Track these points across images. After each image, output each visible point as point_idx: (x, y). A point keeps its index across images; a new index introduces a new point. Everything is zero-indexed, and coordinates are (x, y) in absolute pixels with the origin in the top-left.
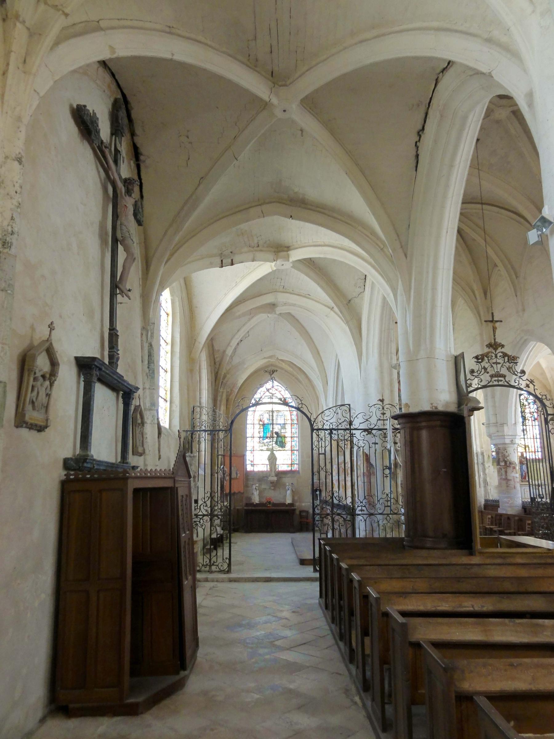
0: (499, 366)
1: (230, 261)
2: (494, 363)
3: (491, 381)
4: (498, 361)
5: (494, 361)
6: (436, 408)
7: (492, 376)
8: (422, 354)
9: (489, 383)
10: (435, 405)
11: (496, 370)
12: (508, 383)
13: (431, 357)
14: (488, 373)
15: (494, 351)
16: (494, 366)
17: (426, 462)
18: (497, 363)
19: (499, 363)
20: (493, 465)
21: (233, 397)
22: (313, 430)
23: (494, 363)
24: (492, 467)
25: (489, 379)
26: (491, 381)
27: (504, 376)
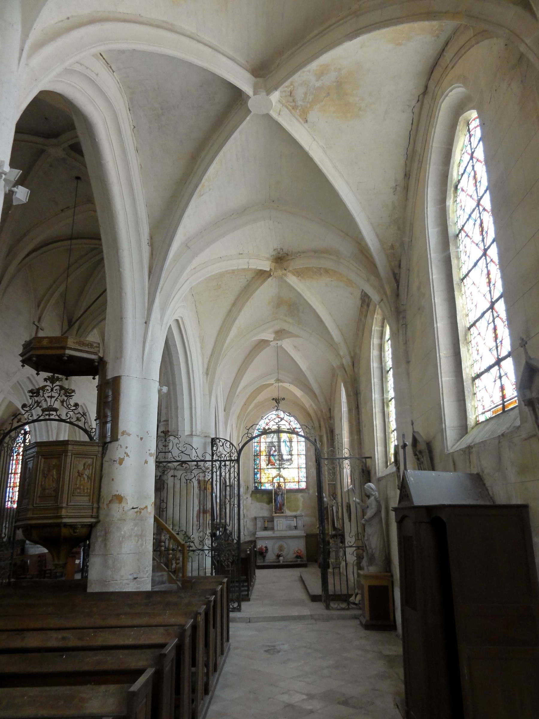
0: (53, 400)
2: (48, 397)
3: (42, 415)
4: (53, 394)
5: (50, 394)
7: (43, 410)
9: (40, 417)
11: (49, 404)
12: (59, 416)
14: (40, 407)
15: (51, 385)
16: (48, 400)
18: (51, 397)
19: (54, 397)
20: (251, 496)
23: (48, 397)
24: (250, 498)
25: (40, 413)
26: (42, 415)
27: (56, 410)
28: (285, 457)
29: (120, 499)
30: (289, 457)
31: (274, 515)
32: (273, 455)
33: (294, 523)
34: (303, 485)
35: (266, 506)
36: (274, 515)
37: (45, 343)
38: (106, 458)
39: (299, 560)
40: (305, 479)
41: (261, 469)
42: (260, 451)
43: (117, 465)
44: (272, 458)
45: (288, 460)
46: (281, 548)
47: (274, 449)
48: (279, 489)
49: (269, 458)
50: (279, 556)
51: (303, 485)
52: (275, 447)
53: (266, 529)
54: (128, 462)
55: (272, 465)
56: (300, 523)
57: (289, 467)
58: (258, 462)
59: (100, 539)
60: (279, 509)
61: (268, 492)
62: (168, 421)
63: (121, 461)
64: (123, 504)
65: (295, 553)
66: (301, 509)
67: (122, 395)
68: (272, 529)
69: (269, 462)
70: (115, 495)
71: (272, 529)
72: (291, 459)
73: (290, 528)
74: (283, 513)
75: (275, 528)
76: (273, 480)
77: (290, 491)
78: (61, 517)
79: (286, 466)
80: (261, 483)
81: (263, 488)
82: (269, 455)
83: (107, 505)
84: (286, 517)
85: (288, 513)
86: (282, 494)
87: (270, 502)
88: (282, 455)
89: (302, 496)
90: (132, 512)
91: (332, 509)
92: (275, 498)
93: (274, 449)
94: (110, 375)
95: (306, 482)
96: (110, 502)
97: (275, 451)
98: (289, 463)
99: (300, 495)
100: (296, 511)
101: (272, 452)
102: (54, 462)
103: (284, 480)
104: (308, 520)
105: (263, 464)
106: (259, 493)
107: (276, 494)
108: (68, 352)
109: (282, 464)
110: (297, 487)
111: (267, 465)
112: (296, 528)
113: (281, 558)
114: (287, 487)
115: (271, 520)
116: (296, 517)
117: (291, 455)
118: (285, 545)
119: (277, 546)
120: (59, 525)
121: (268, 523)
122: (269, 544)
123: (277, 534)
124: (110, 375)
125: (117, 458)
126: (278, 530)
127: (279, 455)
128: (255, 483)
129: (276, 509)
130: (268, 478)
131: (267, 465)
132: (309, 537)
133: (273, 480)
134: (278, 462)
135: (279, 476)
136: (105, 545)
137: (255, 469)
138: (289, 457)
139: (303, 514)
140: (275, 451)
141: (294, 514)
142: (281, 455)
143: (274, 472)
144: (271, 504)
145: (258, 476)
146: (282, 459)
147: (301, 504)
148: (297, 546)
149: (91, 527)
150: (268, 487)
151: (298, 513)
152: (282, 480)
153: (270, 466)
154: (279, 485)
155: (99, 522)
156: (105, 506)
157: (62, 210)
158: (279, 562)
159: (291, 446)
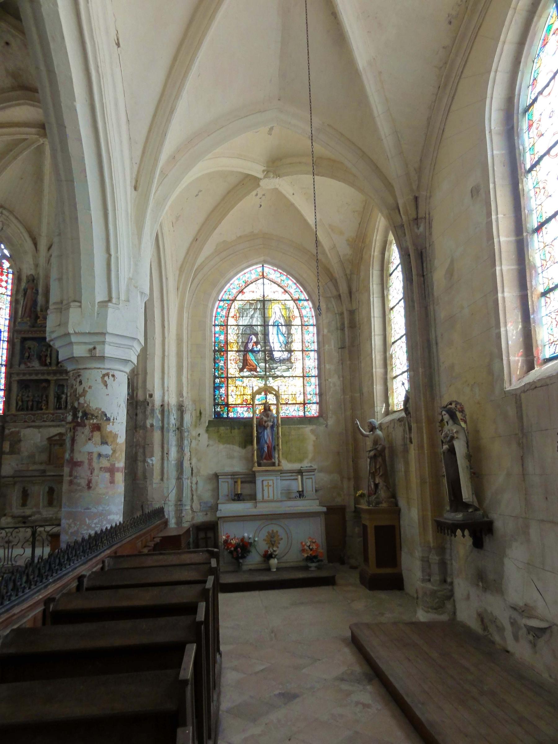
20: (207, 431)
24: (206, 436)
28: (277, 355)
30: (286, 355)
31: (256, 468)
32: (252, 351)
33: (296, 486)
34: (313, 410)
35: (237, 451)
36: (256, 468)
39: (313, 565)
40: (316, 399)
41: (227, 378)
42: (226, 343)
44: (251, 356)
45: (282, 361)
46: (272, 539)
47: (254, 339)
48: (267, 416)
49: (245, 356)
50: (268, 556)
51: (313, 410)
52: (256, 335)
53: (238, 498)
55: (250, 370)
56: (309, 485)
57: (285, 374)
58: (222, 364)
60: (267, 456)
61: (244, 424)
65: (303, 551)
66: (310, 456)
68: (253, 497)
69: (245, 364)
71: (253, 497)
72: (289, 360)
73: (288, 495)
74: (273, 464)
75: (259, 496)
76: (253, 399)
77: (288, 420)
79: (278, 373)
80: (227, 405)
81: (231, 415)
82: (245, 351)
84: (282, 472)
85: (286, 465)
86: (272, 427)
87: (247, 442)
88: (271, 352)
89: (312, 431)
91: (452, 451)
92: (258, 436)
93: (254, 339)
95: (320, 403)
97: (256, 343)
98: (284, 367)
99: (307, 429)
100: (301, 461)
101: (250, 346)
103: (277, 396)
104: (323, 478)
105: (233, 369)
106: (221, 423)
107: (261, 425)
109: (271, 369)
110: (301, 414)
111: (241, 370)
112: (301, 494)
113: (274, 562)
114: (282, 414)
115: (250, 478)
116: (300, 472)
117: (290, 351)
118: (282, 533)
119: (264, 534)
121: (244, 487)
122: (247, 532)
123: (263, 508)
126: (264, 501)
127: (264, 351)
128: (216, 405)
129: (260, 457)
130: (241, 394)
131: (241, 370)
132: (335, 517)
133: (253, 399)
134: (262, 365)
135: (267, 390)
137: (215, 377)
138: (286, 355)
139: (315, 467)
140: (256, 343)
141: (296, 466)
142: (269, 353)
143: (257, 384)
144: (249, 447)
145: (223, 391)
146: (272, 358)
147: (310, 447)
148: (306, 536)
150: (243, 413)
151: (305, 464)
152: (271, 399)
153: (246, 373)
154: (267, 408)
158: (268, 569)
159: (289, 334)
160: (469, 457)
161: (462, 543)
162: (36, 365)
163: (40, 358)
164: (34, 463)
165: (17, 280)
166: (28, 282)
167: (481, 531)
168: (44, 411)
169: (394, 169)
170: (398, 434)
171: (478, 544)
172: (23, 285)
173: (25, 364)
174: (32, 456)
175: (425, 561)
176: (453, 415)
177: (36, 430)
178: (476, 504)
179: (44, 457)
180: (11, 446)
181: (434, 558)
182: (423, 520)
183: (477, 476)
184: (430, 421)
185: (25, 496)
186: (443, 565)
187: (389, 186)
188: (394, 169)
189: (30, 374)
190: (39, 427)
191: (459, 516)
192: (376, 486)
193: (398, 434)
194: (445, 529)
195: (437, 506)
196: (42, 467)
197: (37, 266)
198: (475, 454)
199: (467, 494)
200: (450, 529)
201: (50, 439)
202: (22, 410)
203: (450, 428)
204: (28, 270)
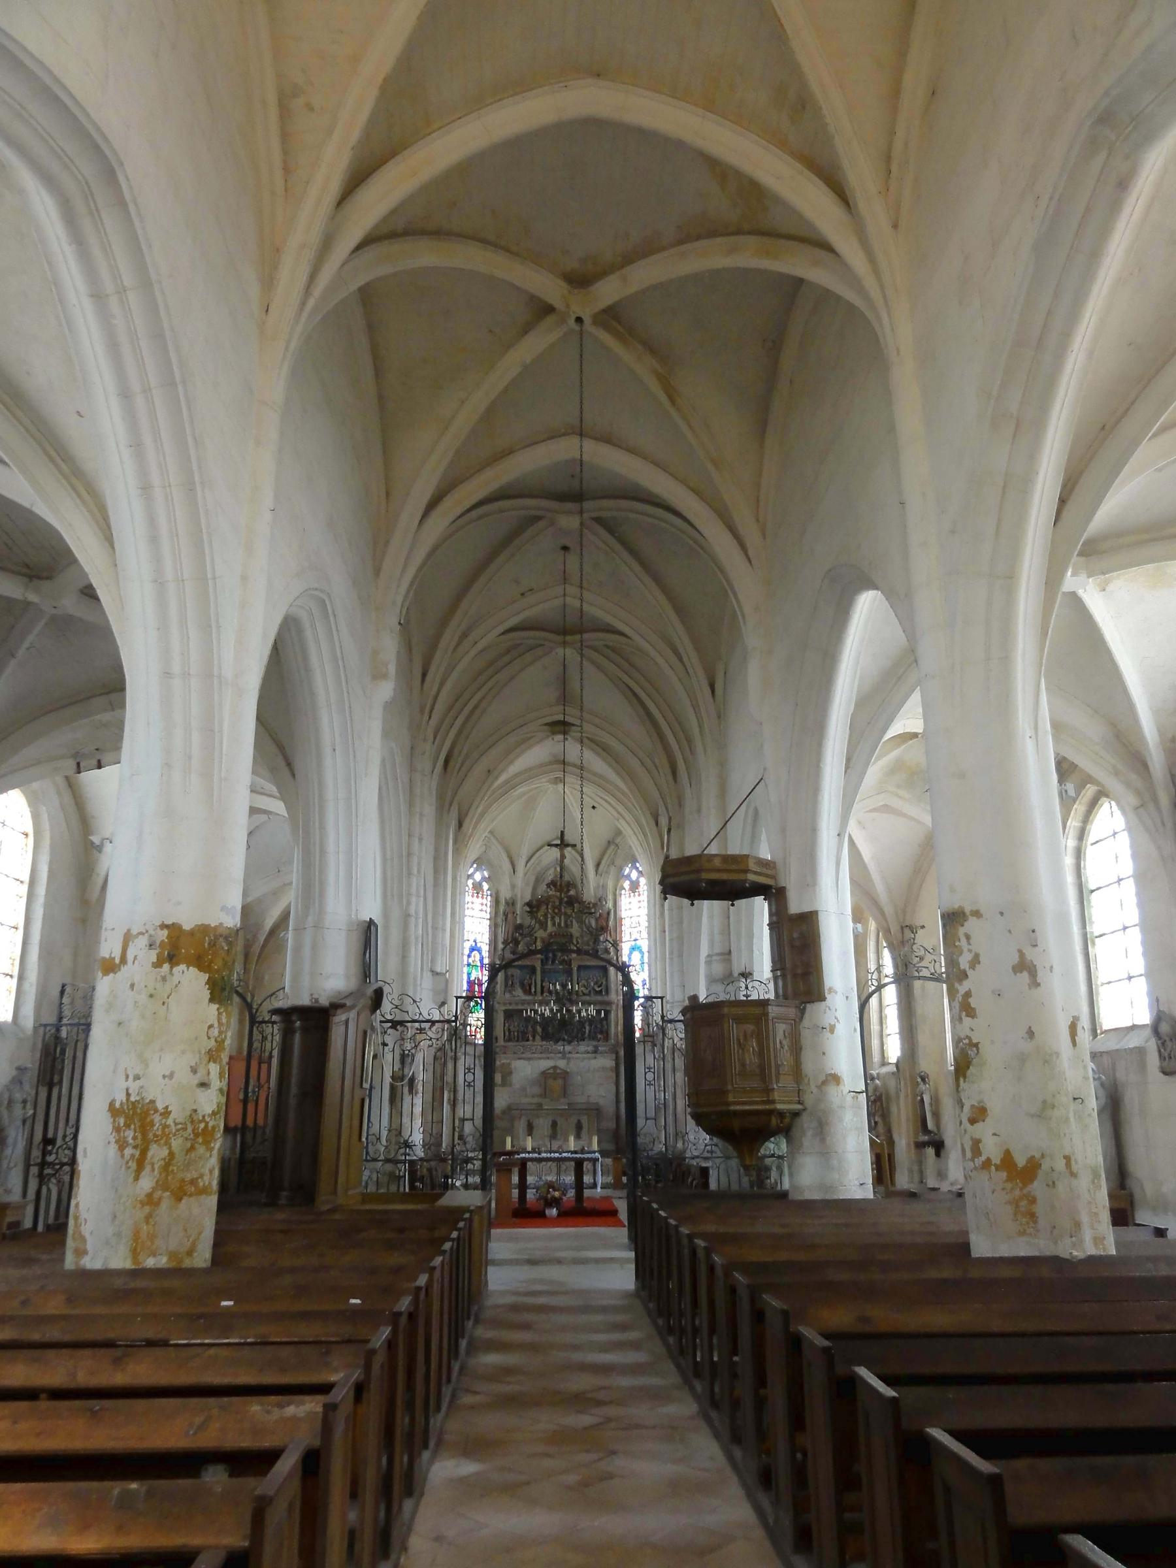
1: (95, 763)
6: (317, 1001)
8: (310, 921)
10: (315, 996)
13: (318, 926)
17: (294, 1080)
21: (256, 949)
22: (253, 1021)
29: (836, 1079)
37: (717, 863)
38: (806, 1022)
43: (827, 1034)
54: (841, 1029)
59: (809, 1133)
62: (730, 953)
63: (832, 1029)
64: (841, 1087)
67: (822, 938)
70: (831, 1075)
78: (773, 1102)
83: (819, 1087)
90: (849, 1097)
91: (922, 1101)
94: (795, 906)
96: (824, 1083)
102: (750, 1027)
108: (751, 877)
120: (771, 1112)
124: (795, 906)
125: (827, 1026)
136: (823, 1140)
149: (796, 1114)
155: (804, 1110)
156: (815, 1090)
157: (523, 594)
160: (931, 1104)
161: (930, 1151)
162: (519, 992)
163: (522, 985)
164: (526, 1096)
165: (496, 901)
166: (507, 903)
167: (939, 1147)
168: (530, 1043)
169: (888, 910)
170: (892, 1084)
171: (938, 1154)
172: (502, 908)
173: (510, 992)
174: (524, 1089)
175: (911, 1171)
176: (923, 1079)
177: (526, 1062)
178: (935, 1130)
179: (537, 1090)
180: (504, 1078)
181: (916, 1168)
182: (908, 1145)
183: (936, 1115)
184: (913, 1078)
185: (530, 1129)
186: (921, 1172)
187: (882, 913)
188: (888, 910)
189: (517, 1004)
190: (529, 1059)
191: (926, 1138)
192: (876, 1123)
193: (892, 1084)
194: (920, 1146)
195: (916, 1135)
196: (536, 1100)
197: (513, 886)
198: (936, 1101)
199: (930, 1125)
200: (920, 1146)
201: (544, 1073)
202: (509, 1040)
203: (922, 1087)
204: (506, 894)
